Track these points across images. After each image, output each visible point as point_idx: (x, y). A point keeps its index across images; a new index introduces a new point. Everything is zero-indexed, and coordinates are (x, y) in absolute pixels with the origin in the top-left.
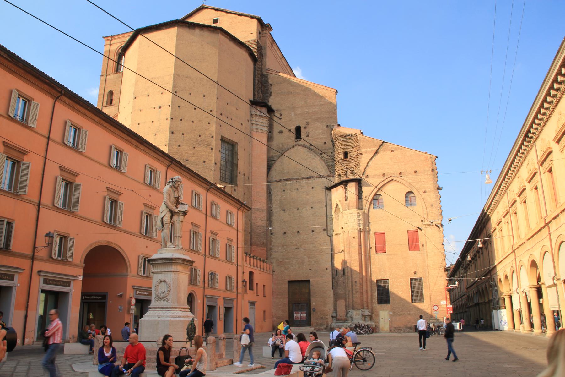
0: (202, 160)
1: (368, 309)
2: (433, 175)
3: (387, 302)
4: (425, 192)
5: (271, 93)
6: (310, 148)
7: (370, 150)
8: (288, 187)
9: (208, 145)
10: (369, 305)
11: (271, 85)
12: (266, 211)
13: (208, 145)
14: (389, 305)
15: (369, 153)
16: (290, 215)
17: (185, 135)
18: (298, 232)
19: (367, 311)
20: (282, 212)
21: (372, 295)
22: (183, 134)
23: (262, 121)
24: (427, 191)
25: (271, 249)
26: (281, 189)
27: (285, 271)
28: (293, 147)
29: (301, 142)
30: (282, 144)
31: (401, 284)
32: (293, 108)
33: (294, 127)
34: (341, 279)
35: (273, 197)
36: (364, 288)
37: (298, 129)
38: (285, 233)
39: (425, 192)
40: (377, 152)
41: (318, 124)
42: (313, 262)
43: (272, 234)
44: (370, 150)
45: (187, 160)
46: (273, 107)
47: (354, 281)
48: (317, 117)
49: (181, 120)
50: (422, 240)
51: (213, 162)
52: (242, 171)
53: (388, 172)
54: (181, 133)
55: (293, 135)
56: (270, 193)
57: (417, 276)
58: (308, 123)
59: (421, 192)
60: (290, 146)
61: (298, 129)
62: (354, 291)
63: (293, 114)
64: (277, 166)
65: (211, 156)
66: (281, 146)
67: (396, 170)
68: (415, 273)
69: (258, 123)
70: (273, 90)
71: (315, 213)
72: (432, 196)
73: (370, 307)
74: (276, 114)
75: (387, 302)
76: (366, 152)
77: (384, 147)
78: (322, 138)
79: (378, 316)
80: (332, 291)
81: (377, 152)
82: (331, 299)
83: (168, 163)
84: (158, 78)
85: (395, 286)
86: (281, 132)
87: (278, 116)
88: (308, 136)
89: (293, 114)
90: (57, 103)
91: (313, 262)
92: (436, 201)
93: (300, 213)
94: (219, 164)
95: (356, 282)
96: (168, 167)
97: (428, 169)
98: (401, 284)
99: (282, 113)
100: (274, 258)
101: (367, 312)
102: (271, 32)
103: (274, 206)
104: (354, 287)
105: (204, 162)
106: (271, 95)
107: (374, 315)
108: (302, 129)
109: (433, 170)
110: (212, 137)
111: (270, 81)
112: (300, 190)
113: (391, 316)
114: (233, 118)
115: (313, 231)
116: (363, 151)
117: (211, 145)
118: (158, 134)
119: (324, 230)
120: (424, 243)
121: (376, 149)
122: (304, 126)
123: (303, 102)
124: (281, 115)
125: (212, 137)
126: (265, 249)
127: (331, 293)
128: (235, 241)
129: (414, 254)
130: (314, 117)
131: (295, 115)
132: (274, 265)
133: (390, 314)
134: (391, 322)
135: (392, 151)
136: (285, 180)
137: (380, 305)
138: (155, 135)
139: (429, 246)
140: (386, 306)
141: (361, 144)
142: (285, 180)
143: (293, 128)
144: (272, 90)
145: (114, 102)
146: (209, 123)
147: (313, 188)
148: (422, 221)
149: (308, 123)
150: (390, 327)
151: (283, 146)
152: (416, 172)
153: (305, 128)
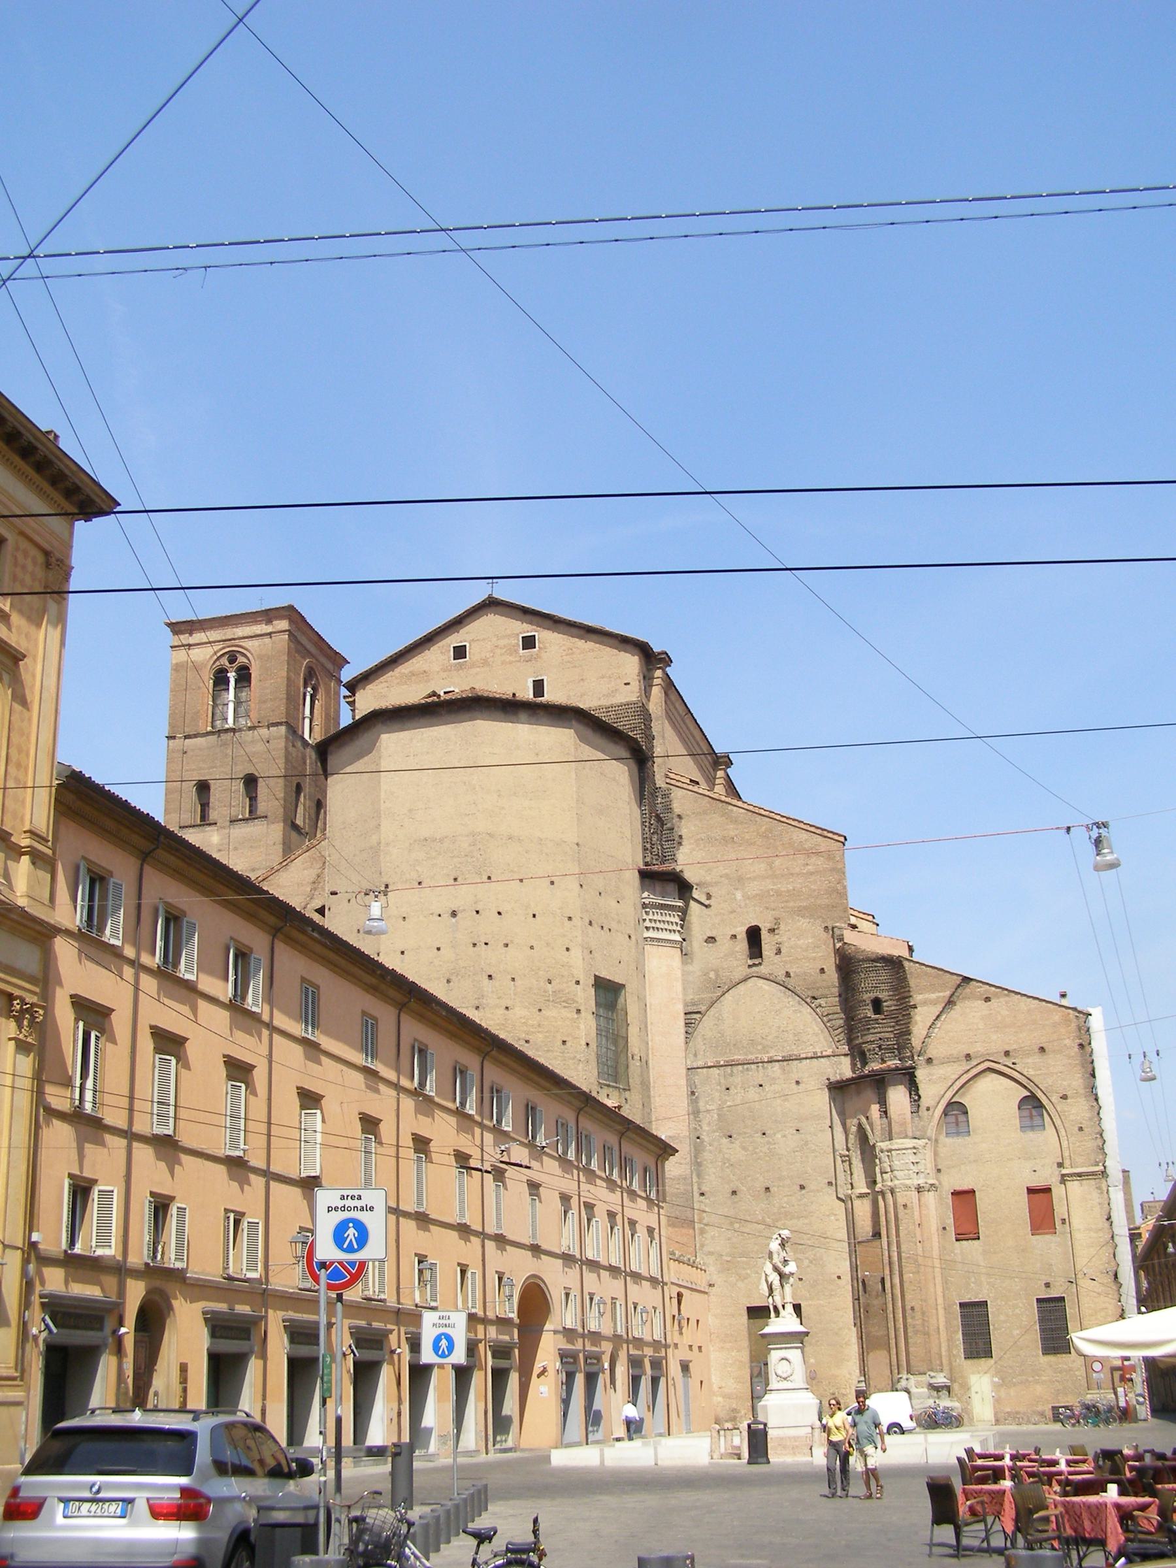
0: (559, 1039)
1: (942, 1371)
2: (1082, 1055)
3: (988, 1354)
4: (1064, 1097)
5: (681, 837)
6: (785, 983)
7: (933, 996)
8: (737, 1079)
9: (568, 1002)
10: (945, 1361)
11: (679, 816)
12: (688, 1141)
13: (568, 1002)
14: (991, 1362)
15: (934, 1003)
16: (744, 1148)
17: (518, 982)
18: (767, 1189)
19: (942, 1375)
20: (725, 1141)
21: (950, 1340)
22: (513, 979)
23: (668, 918)
24: (1069, 1094)
25: (702, 1232)
26: (719, 1084)
27: (740, 1284)
28: (745, 980)
29: (763, 970)
30: (716, 971)
31: (1017, 1311)
32: (740, 879)
33: (745, 929)
34: (876, 1302)
35: (701, 1104)
36: (933, 1321)
37: (754, 935)
38: (734, 1193)
39: (1064, 1097)
40: (950, 1003)
41: (803, 923)
42: (806, 1262)
43: (702, 1194)
44: (933, 996)
45: (527, 1042)
46: (690, 875)
47: (908, 1307)
48: (798, 904)
49: (506, 945)
50: (1060, 1211)
51: (584, 1043)
52: (636, 1051)
53: (977, 1048)
54: (509, 977)
55: (742, 945)
56: (693, 1093)
57: (1054, 1294)
58: (777, 921)
59: (1055, 1098)
60: (738, 975)
61: (754, 935)
62: (910, 1330)
63: (739, 895)
64: (706, 1026)
65: (578, 1028)
66: (712, 975)
67: (995, 1043)
68: (1047, 1285)
69: (658, 925)
70: (685, 829)
71: (806, 1143)
72: (1077, 1110)
73: (946, 1368)
74: (696, 894)
75: (988, 1354)
76: (925, 1003)
77: (967, 990)
78: (814, 959)
79: (966, 1387)
80: (854, 1329)
81: (950, 1003)
82: (854, 1349)
83: (578, 1104)
84: (441, 841)
85: (1002, 1318)
86: (711, 940)
87: (703, 899)
88: (779, 952)
89: (739, 895)
90: (402, 1014)
91: (806, 1262)
92: (1091, 1119)
93: (769, 1143)
94: (593, 1045)
95: (912, 1309)
96: (579, 1111)
97: (1071, 1043)
98: (1017, 1311)
99: (713, 891)
100: (710, 1253)
101: (941, 1379)
102: (668, 669)
103: (706, 1128)
104: (909, 1320)
105: (564, 1042)
106: (680, 844)
107: (956, 1387)
108: (764, 934)
109: (1081, 1046)
110: (578, 983)
111: (677, 807)
112: (767, 1087)
113: (996, 1387)
114: (614, 926)
115: (802, 1187)
116: (917, 998)
117: (575, 1002)
118: (453, 978)
119: (830, 1183)
120: (1066, 1217)
121: (948, 993)
122: (769, 926)
123: (763, 866)
124: (709, 896)
125: (578, 983)
126: (691, 1231)
127: (852, 1335)
128: (657, 1231)
129: (1043, 1242)
130: (791, 904)
131: (746, 897)
132: (711, 1269)
133: (992, 1382)
134: (997, 1401)
135: (987, 999)
136: (730, 1064)
137: (970, 1362)
138: (448, 981)
139: (1076, 1222)
140: (984, 1363)
141: (912, 982)
142: (730, 1064)
143: (741, 931)
144: (684, 831)
145: (213, 815)
146: (568, 949)
147: (798, 1083)
148: (1060, 1165)
149: (777, 921)
150: (995, 1414)
151: (717, 975)
152: (1042, 1049)
153: (772, 931)
